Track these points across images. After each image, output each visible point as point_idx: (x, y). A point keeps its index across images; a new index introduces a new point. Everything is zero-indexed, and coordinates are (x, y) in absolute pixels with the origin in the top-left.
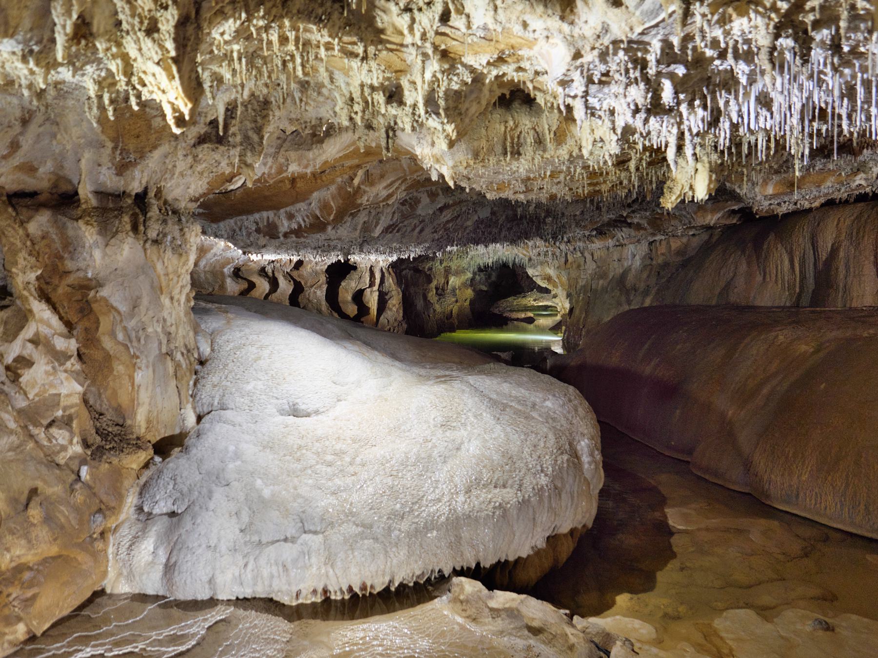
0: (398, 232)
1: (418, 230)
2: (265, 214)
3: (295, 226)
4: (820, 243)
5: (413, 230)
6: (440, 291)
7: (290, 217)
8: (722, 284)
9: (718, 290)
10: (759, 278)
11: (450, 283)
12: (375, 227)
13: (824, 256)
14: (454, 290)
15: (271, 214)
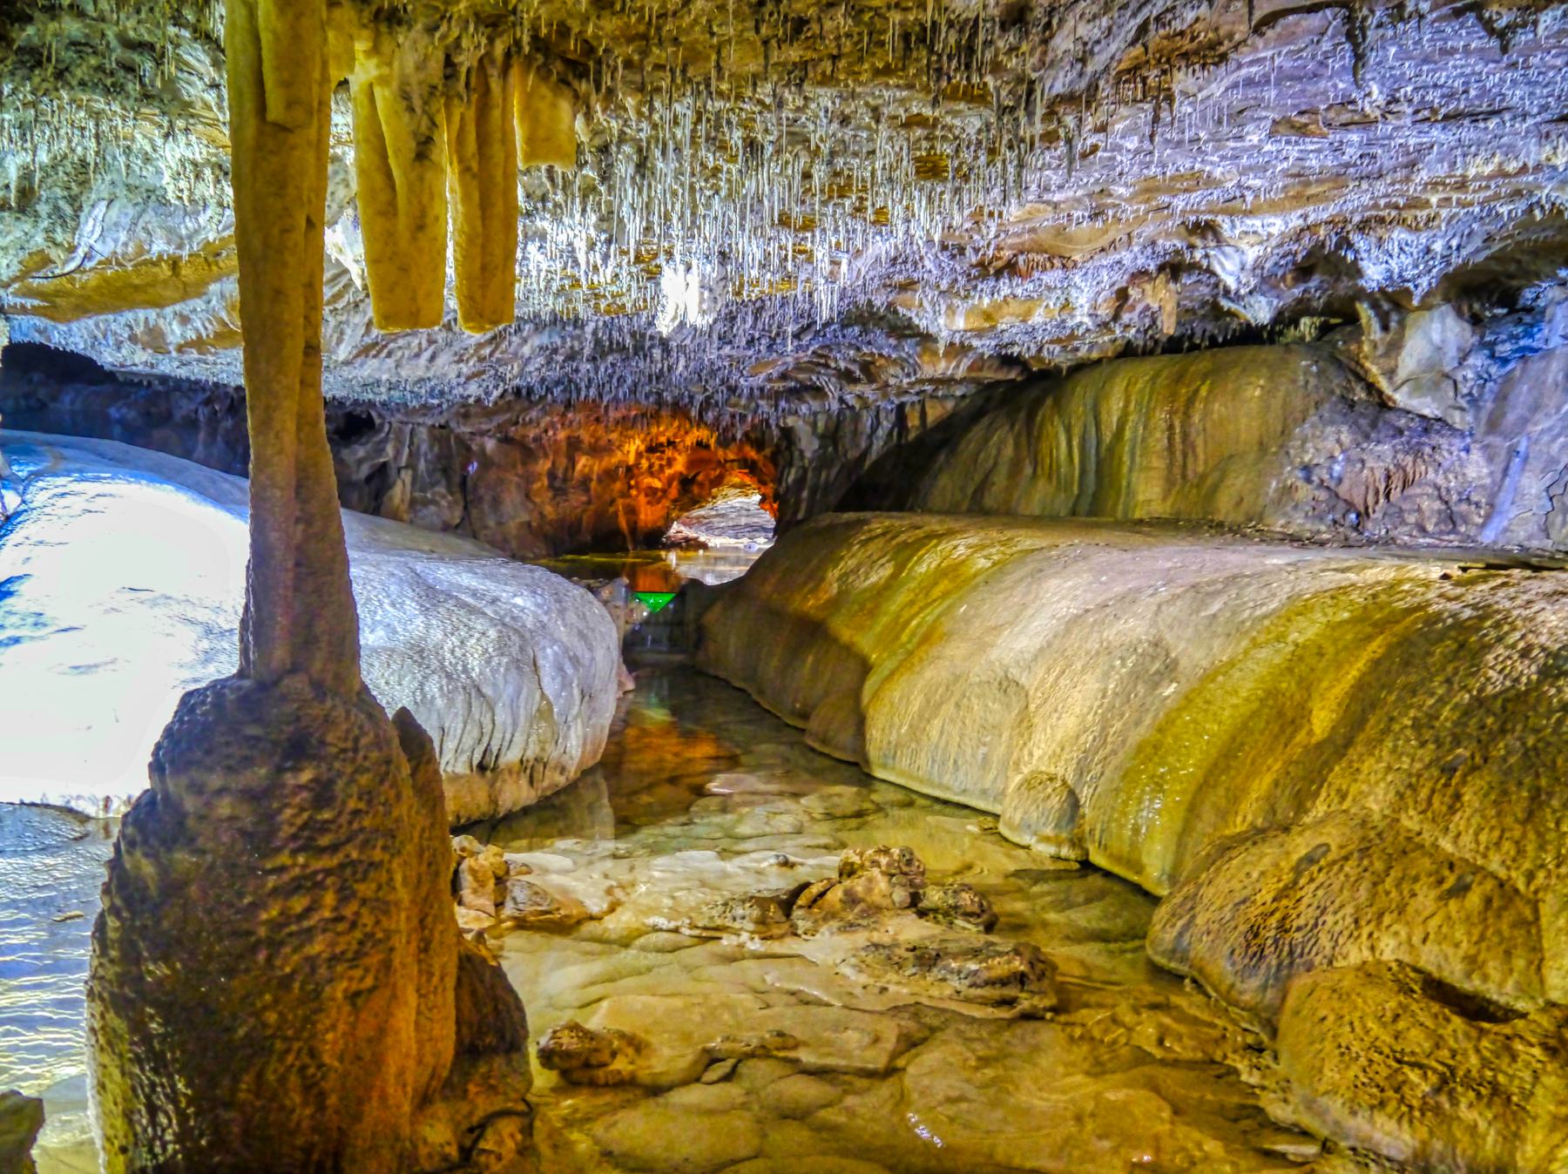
0: (389, 355)
1: (426, 355)
2: (141, 314)
3: (191, 335)
4: (1104, 416)
5: (417, 355)
6: (557, 484)
7: (185, 320)
8: (978, 478)
9: (970, 491)
10: (1028, 470)
11: (579, 467)
12: (338, 343)
13: (1107, 437)
14: (585, 481)
15: (152, 314)
